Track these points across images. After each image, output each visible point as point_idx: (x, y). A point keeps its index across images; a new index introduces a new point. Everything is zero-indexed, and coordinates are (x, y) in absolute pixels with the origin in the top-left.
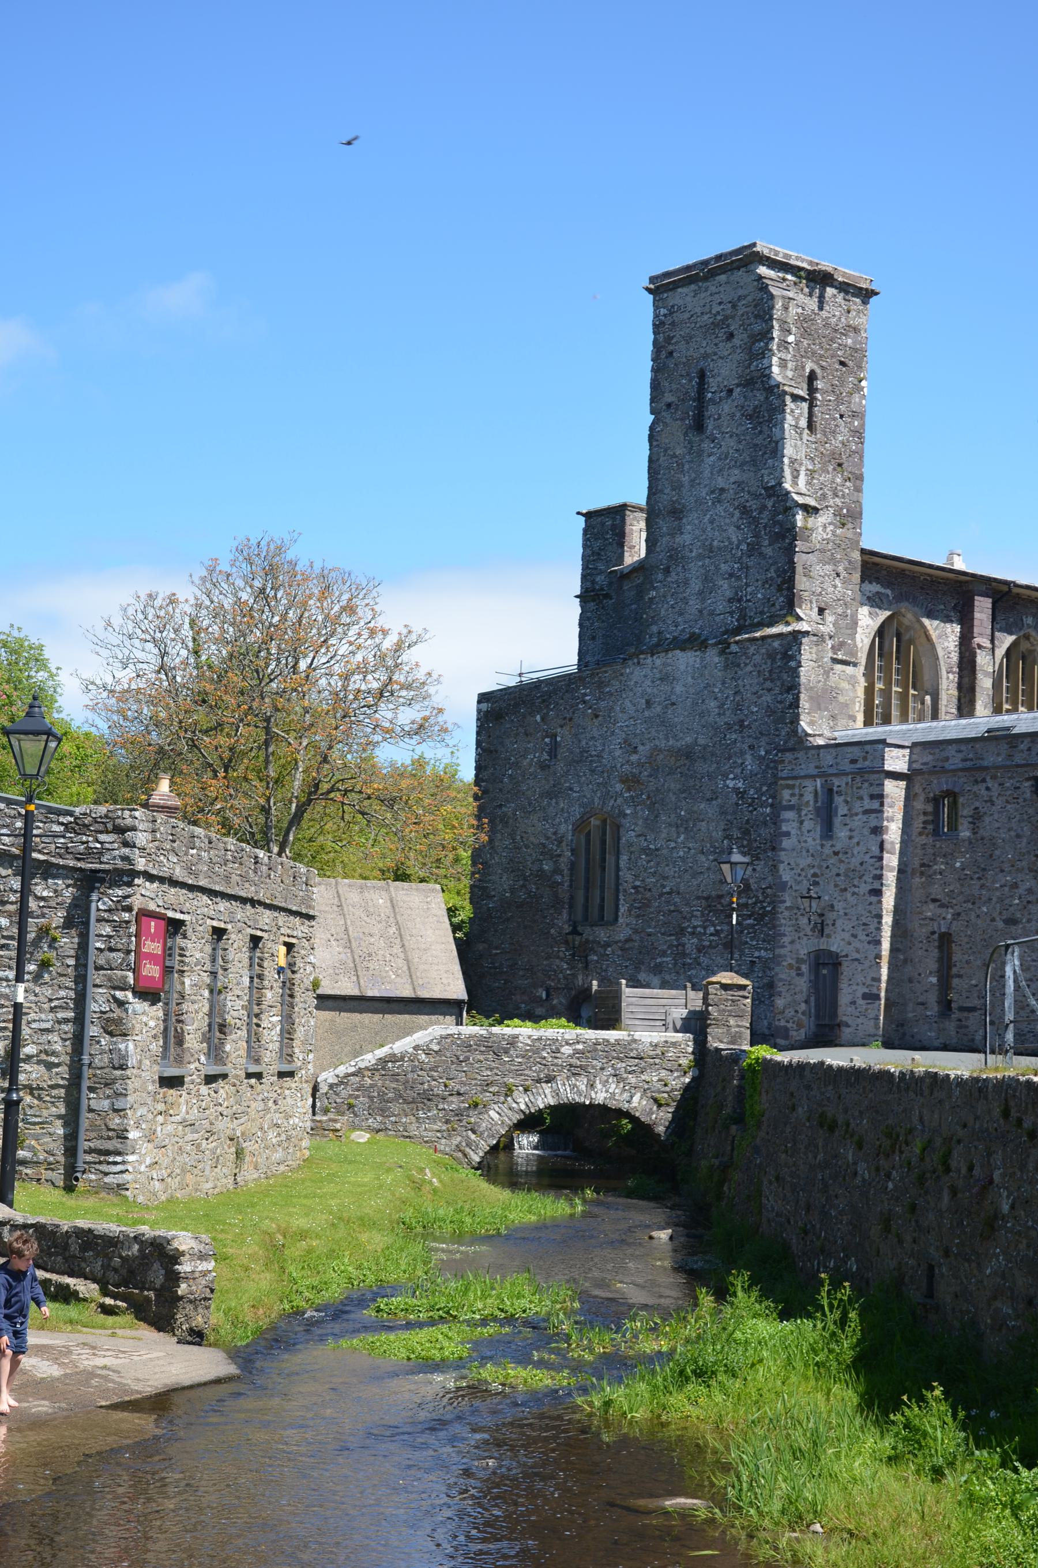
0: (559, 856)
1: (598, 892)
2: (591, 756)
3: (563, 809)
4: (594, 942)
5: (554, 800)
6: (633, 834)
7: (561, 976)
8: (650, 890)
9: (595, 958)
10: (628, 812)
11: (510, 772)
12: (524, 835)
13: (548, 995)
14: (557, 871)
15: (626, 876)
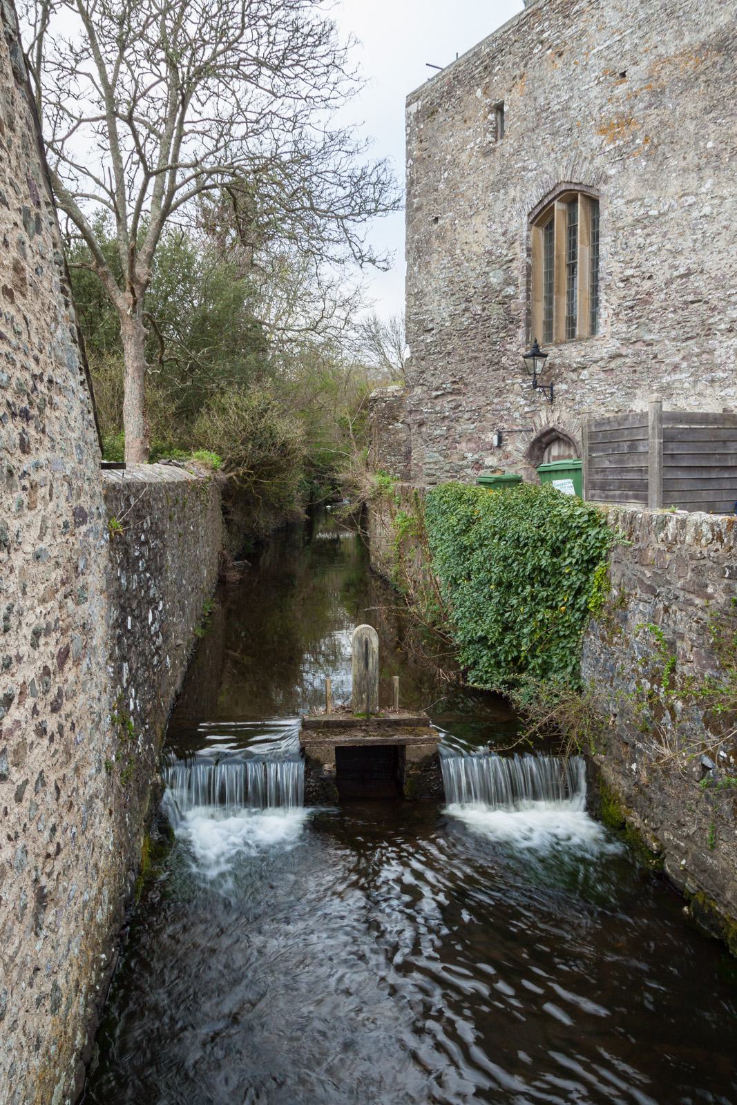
0: (511, 261)
1: (564, 300)
2: (554, 113)
3: (514, 200)
4: (563, 365)
5: (502, 191)
6: (621, 202)
7: (516, 415)
8: (650, 277)
9: (565, 387)
10: (612, 172)
11: (446, 174)
12: (465, 247)
13: (500, 440)
14: (509, 281)
15: (610, 265)
